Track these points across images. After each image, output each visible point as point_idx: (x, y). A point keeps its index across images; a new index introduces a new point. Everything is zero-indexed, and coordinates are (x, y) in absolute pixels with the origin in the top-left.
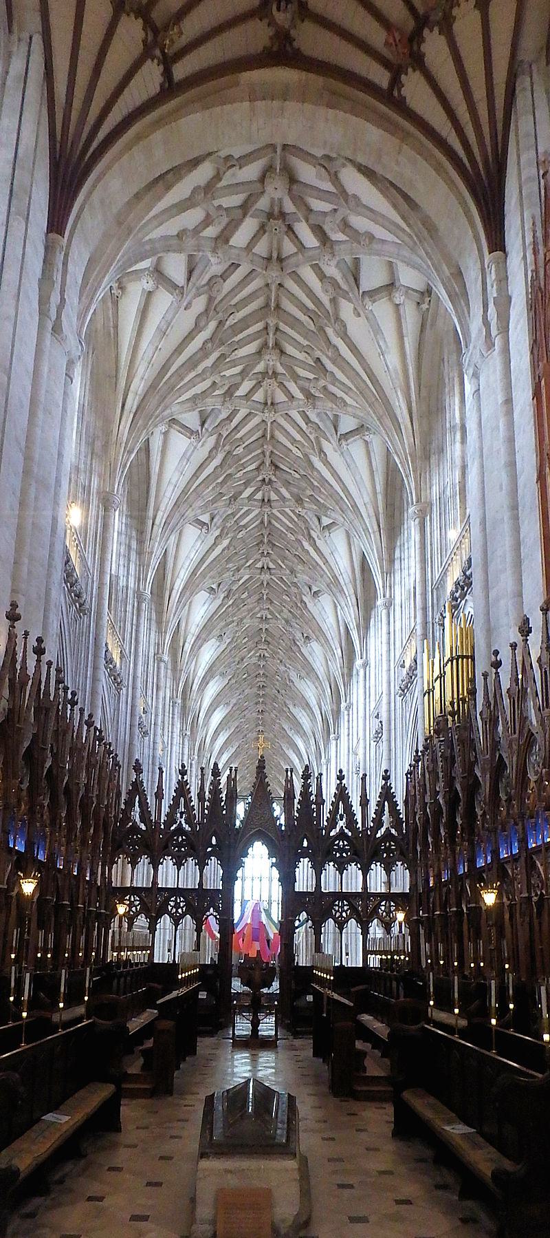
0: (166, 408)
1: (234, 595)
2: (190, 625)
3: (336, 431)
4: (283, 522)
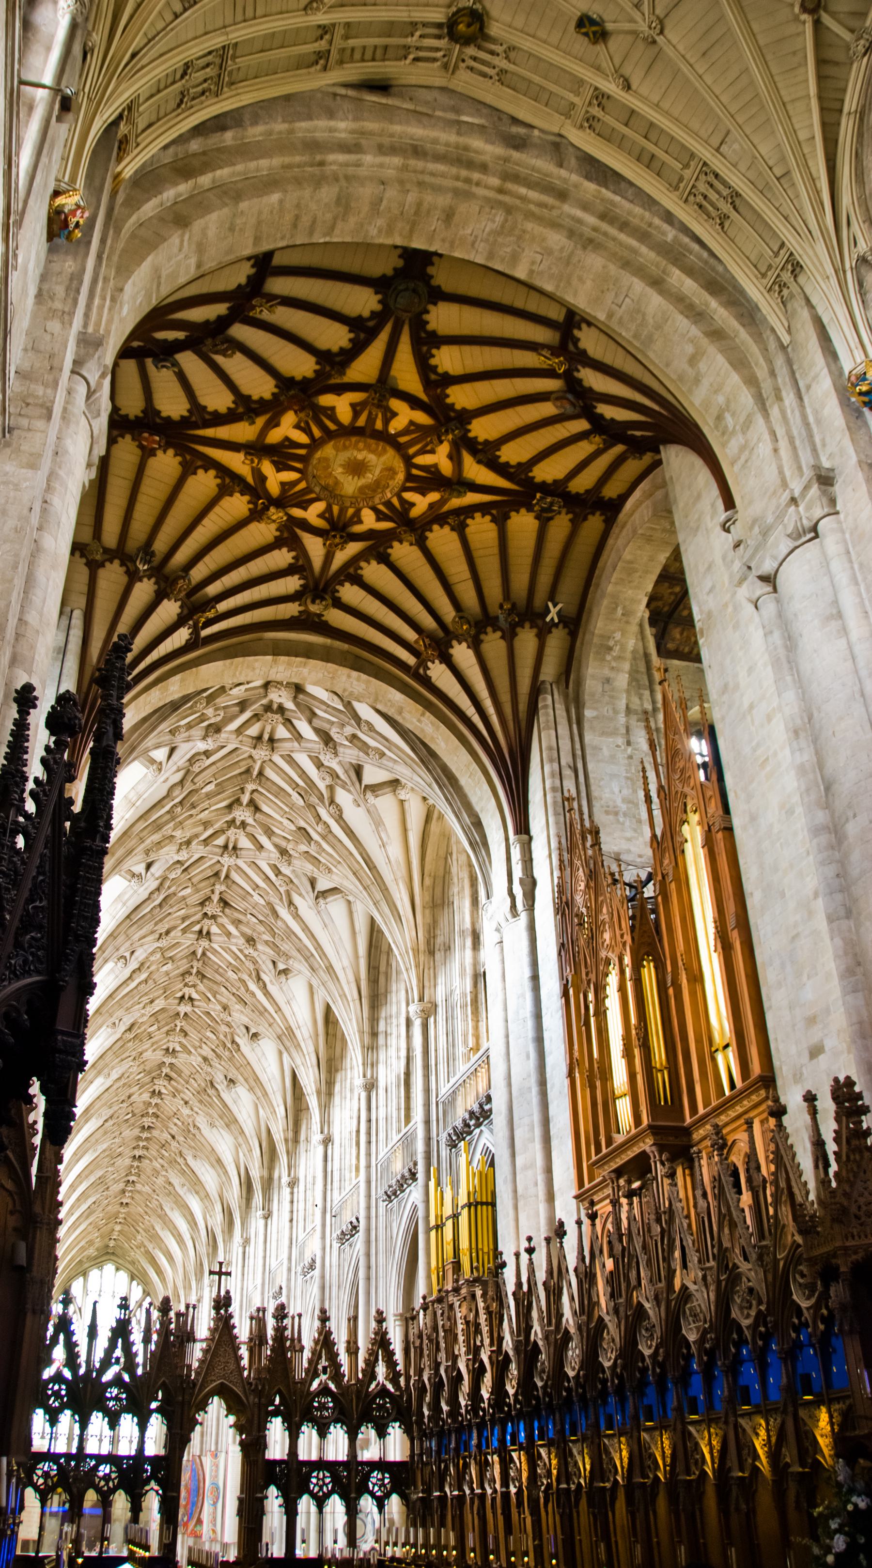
3: (313, 888)
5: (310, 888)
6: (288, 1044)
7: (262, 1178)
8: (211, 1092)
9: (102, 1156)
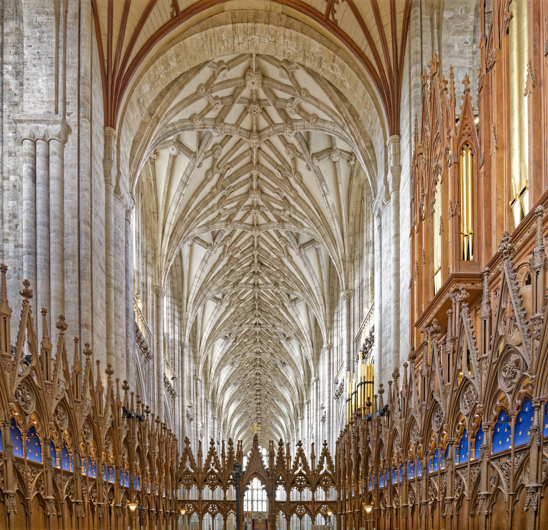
0: (190, 231)
1: (239, 340)
2: (213, 358)
4: (267, 298)
5: (296, 243)
8: (277, 369)
9: (243, 402)
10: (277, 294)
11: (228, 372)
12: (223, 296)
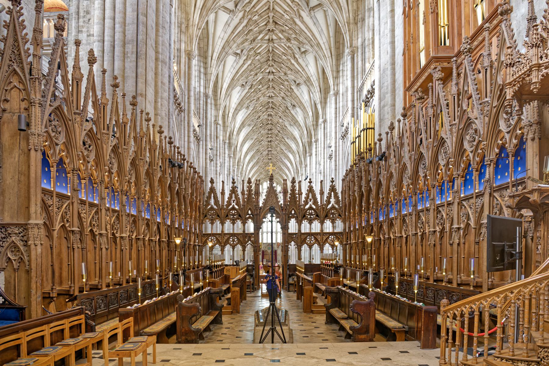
3: (308, 6)
5: (306, 6)
6: (308, 84)
7: (308, 141)
8: (287, 111)
10: (289, 47)
11: (243, 115)
12: (242, 51)
